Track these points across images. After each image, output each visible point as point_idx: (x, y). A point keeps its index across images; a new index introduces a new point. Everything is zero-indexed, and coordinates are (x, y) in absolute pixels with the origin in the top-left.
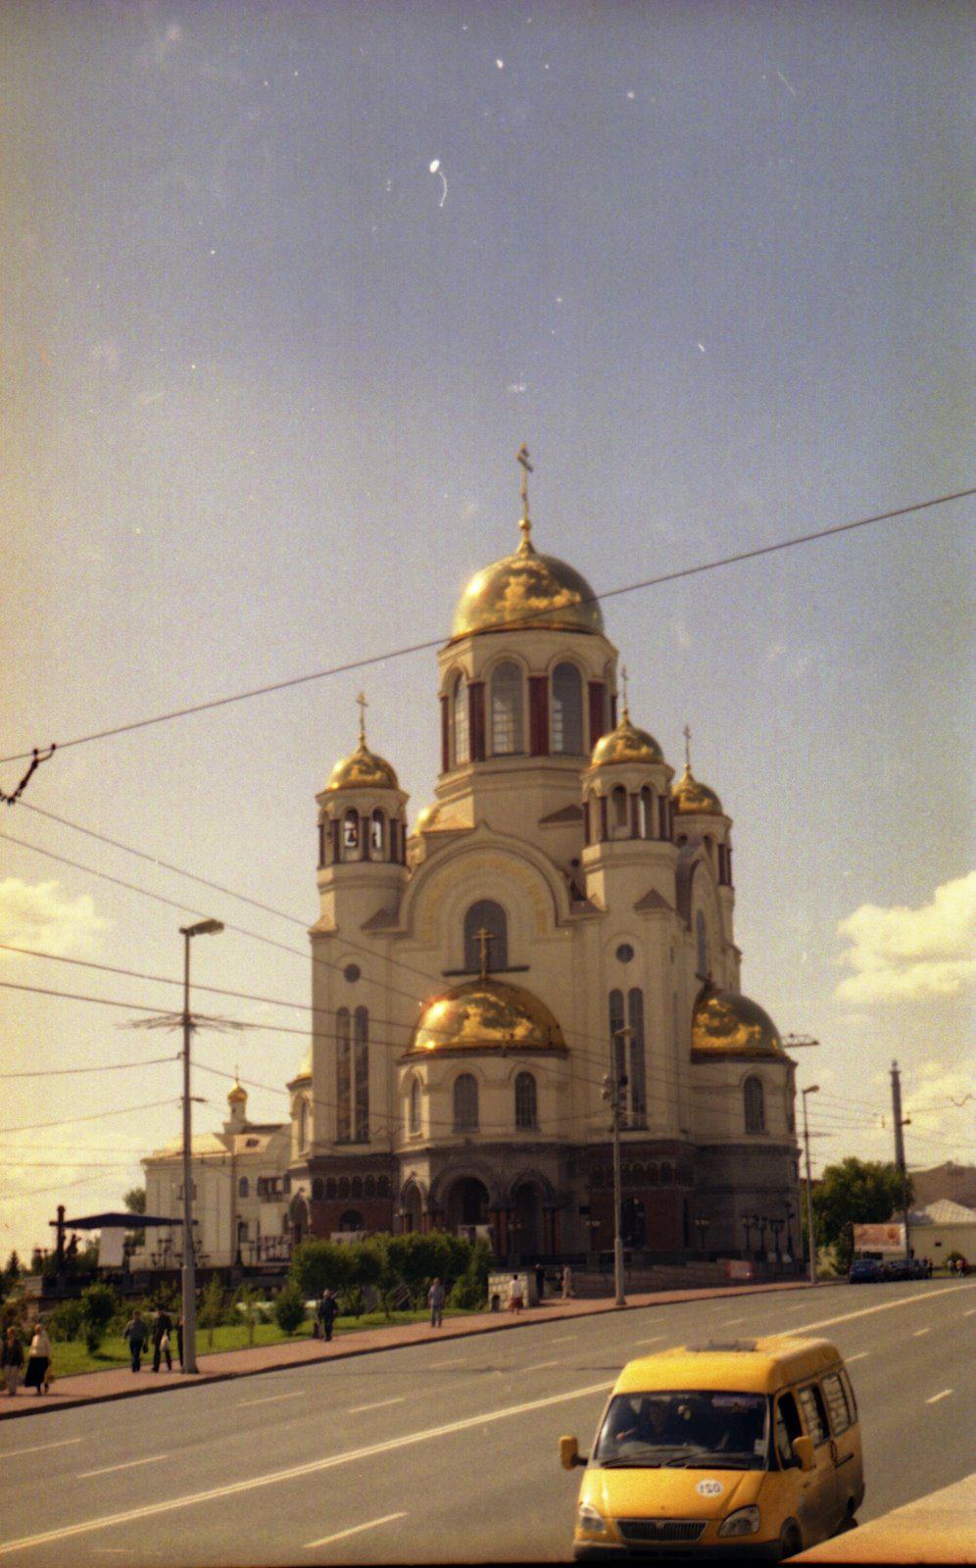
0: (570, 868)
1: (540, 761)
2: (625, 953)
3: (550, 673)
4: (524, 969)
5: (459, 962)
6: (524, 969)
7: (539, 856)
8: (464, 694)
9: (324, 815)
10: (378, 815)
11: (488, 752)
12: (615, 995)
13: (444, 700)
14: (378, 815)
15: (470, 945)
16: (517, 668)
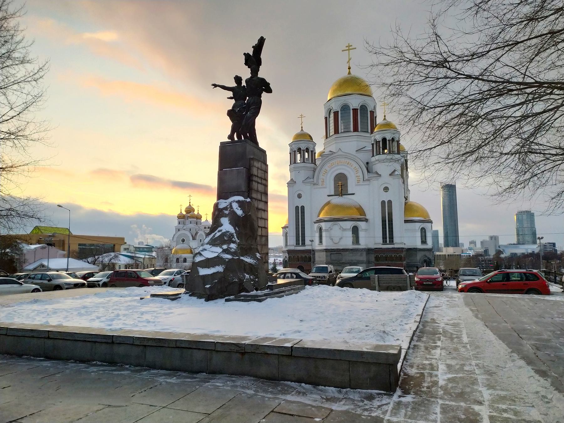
0: (366, 165)
1: (356, 133)
2: (386, 189)
3: (359, 108)
4: (353, 194)
5: (333, 193)
6: (353, 194)
7: (359, 160)
8: (332, 115)
9: (291, 149)
10: (307, 150)
11: (340, 132)
12: (383, 203)
13: (326, 118)
14: (307, 150)
15: (336, 187)
16: (349, 106)
